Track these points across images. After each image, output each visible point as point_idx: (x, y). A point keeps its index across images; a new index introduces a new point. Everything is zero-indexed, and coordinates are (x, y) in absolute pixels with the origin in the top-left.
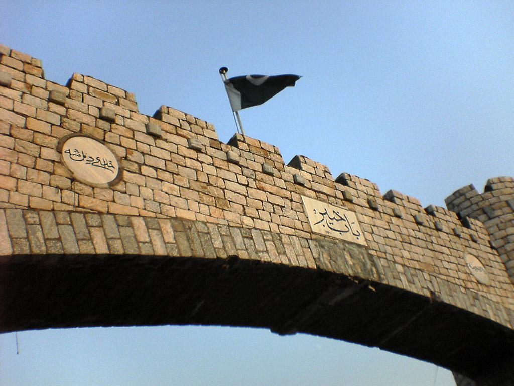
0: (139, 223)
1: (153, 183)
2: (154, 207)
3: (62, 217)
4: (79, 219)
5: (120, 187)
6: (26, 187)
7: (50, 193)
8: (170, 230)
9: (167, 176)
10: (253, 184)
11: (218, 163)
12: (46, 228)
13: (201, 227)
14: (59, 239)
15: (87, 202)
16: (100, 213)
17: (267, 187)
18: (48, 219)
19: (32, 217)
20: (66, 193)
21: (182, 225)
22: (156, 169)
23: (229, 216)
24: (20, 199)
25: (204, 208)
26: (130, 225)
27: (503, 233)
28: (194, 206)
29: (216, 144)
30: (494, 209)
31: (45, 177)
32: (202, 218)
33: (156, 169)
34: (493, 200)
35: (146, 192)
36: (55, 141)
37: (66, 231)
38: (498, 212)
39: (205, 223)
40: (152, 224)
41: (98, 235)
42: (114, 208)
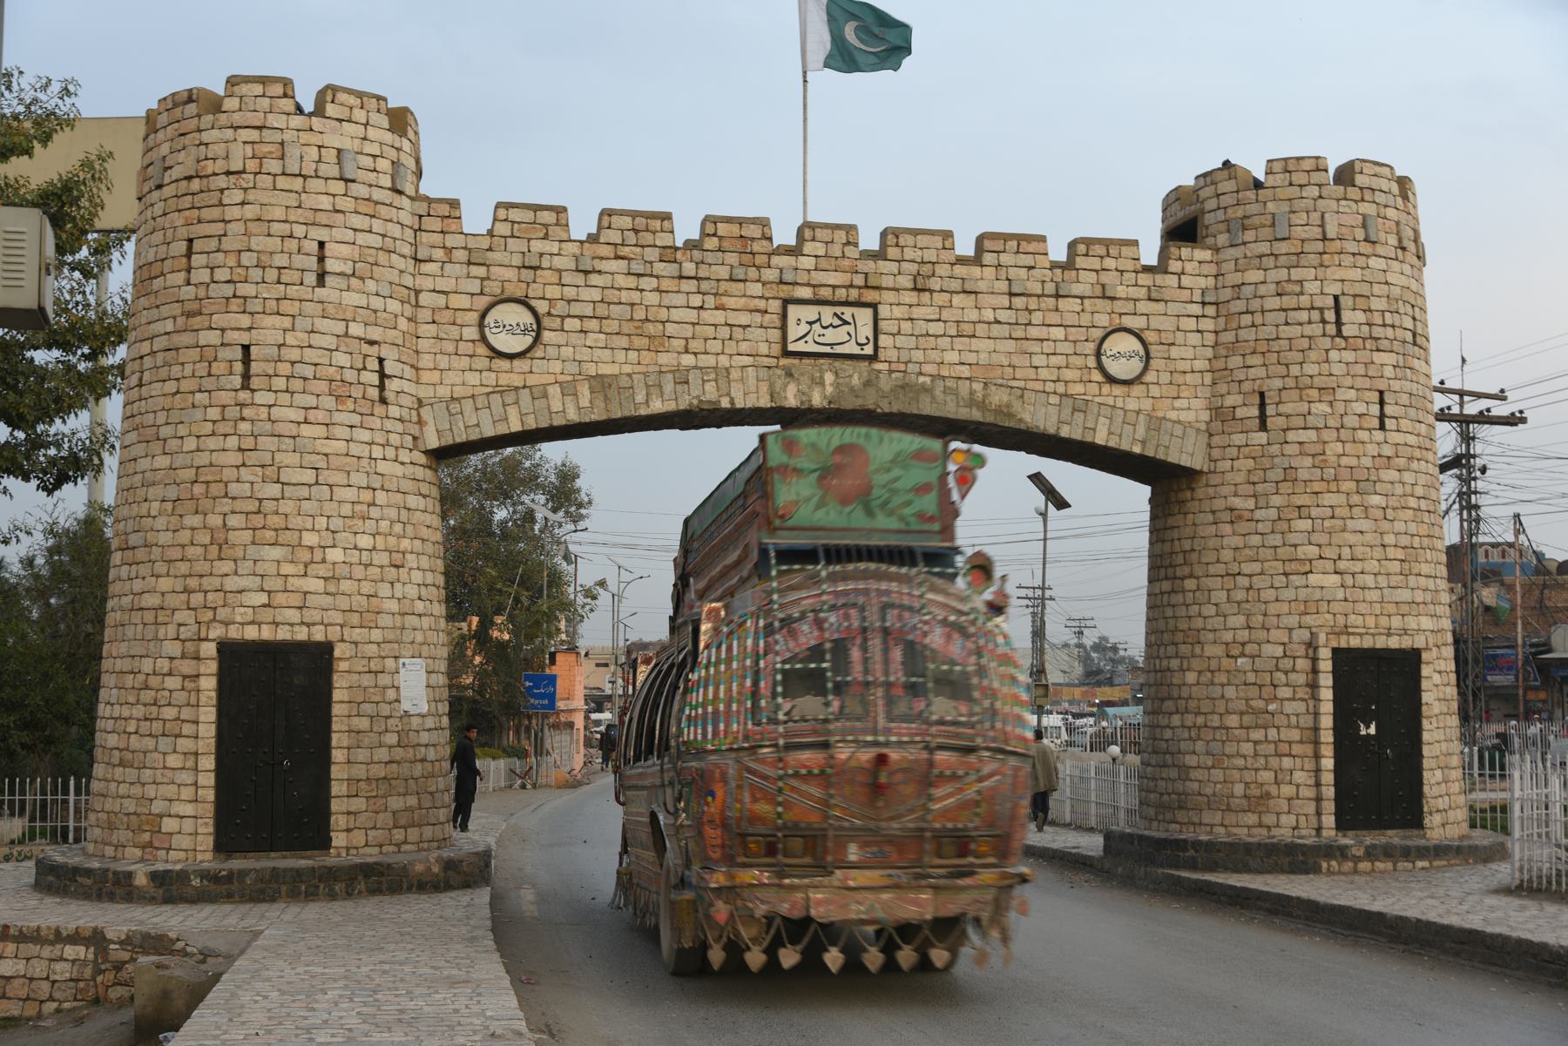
0: (554, 391)
1: (576, 339)
2: (572, 368)
3: (481, 401)
4: (496, 400)
5: (539, 352)
6: (452, 378)
7: (473, 378)
8: (586, 392)
9: (593, 324)
10: (710, 301)
11: (666, 284)
12: (466, 414)
13: (624, 382)
14: (478, 425)
15: (505, 380)
16: (517, 388)
17: (730, 302)
18: (468, 405)
19: (455, 407)
20: (485, 374)
21: (601, 384)
22: (581, 318)
23: (664, 359)
24: (443, 391)
25: (633, 355)
26: (545, 396)
27: (1235, 278)
28: (620, 356)
29: (669, 254)
30: (1244, 228)
31: (465, 362)
32: (627, 369)
33: (581, 318)
34: (1253, 208)
35: (567, 352)
36: (475, 316)
37: (484, 414)
38: (1249, 235)
39: (629, 375)
40: (569, 390)
41: (513, 413)
42: (532, 380)
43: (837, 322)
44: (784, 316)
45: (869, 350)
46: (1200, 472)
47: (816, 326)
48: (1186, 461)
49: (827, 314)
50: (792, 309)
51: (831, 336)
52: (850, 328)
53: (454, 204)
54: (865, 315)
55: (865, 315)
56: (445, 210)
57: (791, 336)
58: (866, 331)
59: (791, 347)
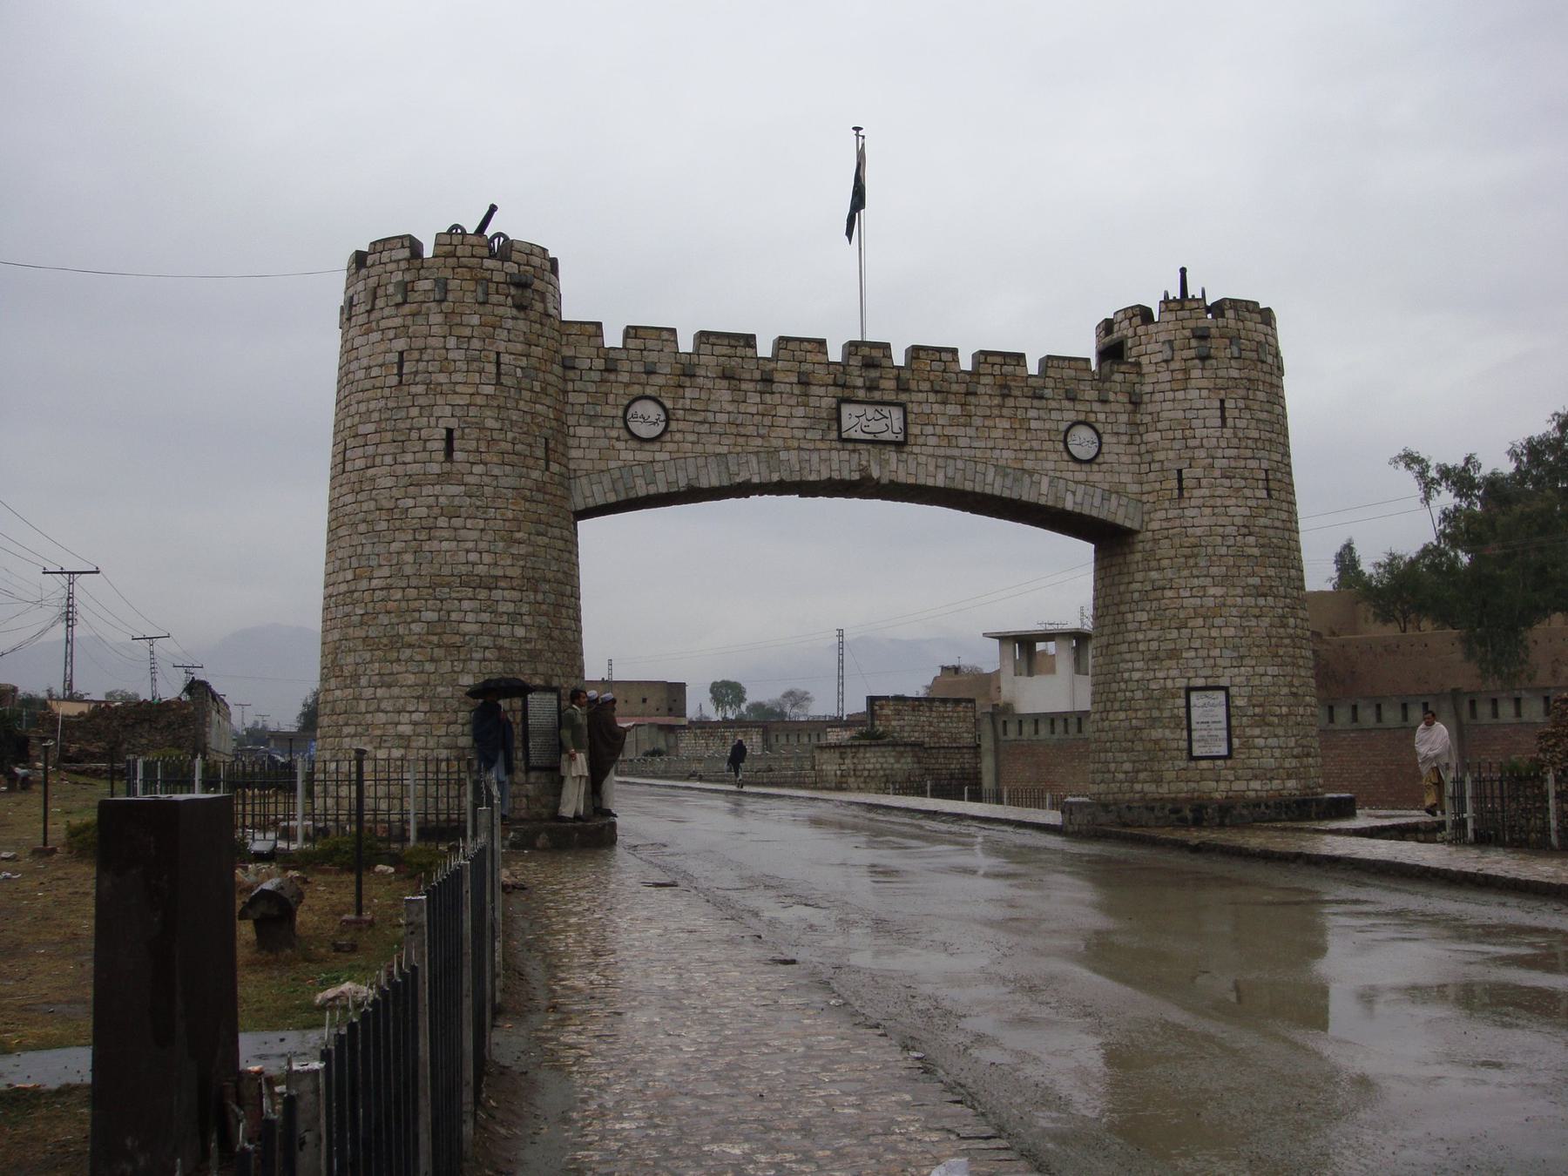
43: (878, 416)
44: (838, 410)
45: (901, 438)
46: (1138, 532)
47: (863, 419)
48: (1128, 524)
49: (870, 411)
50: (846, 410)
51: (874, 426)
52: (888, 421)
53: (599, 325)
54: (897, 414)
55: (897, 414)
56: (592, 329)
57: (845, 427)
58: (897, 424)
59: (844, 435)
